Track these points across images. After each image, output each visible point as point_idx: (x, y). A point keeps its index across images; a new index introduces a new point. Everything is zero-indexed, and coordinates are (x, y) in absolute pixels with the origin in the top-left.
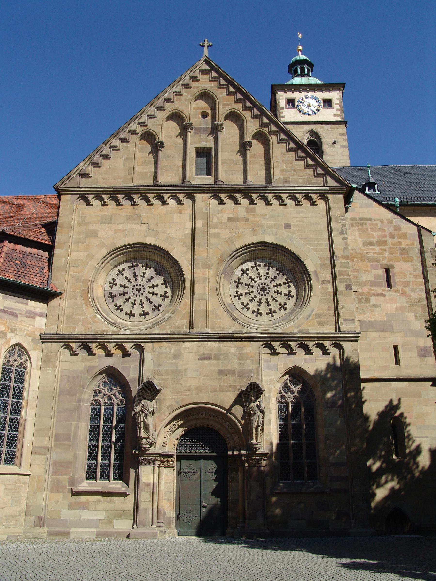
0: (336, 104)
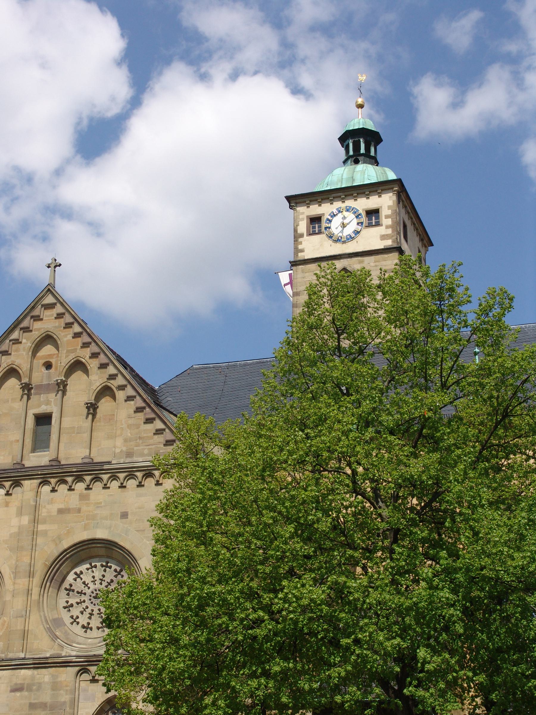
0: (387, 217)
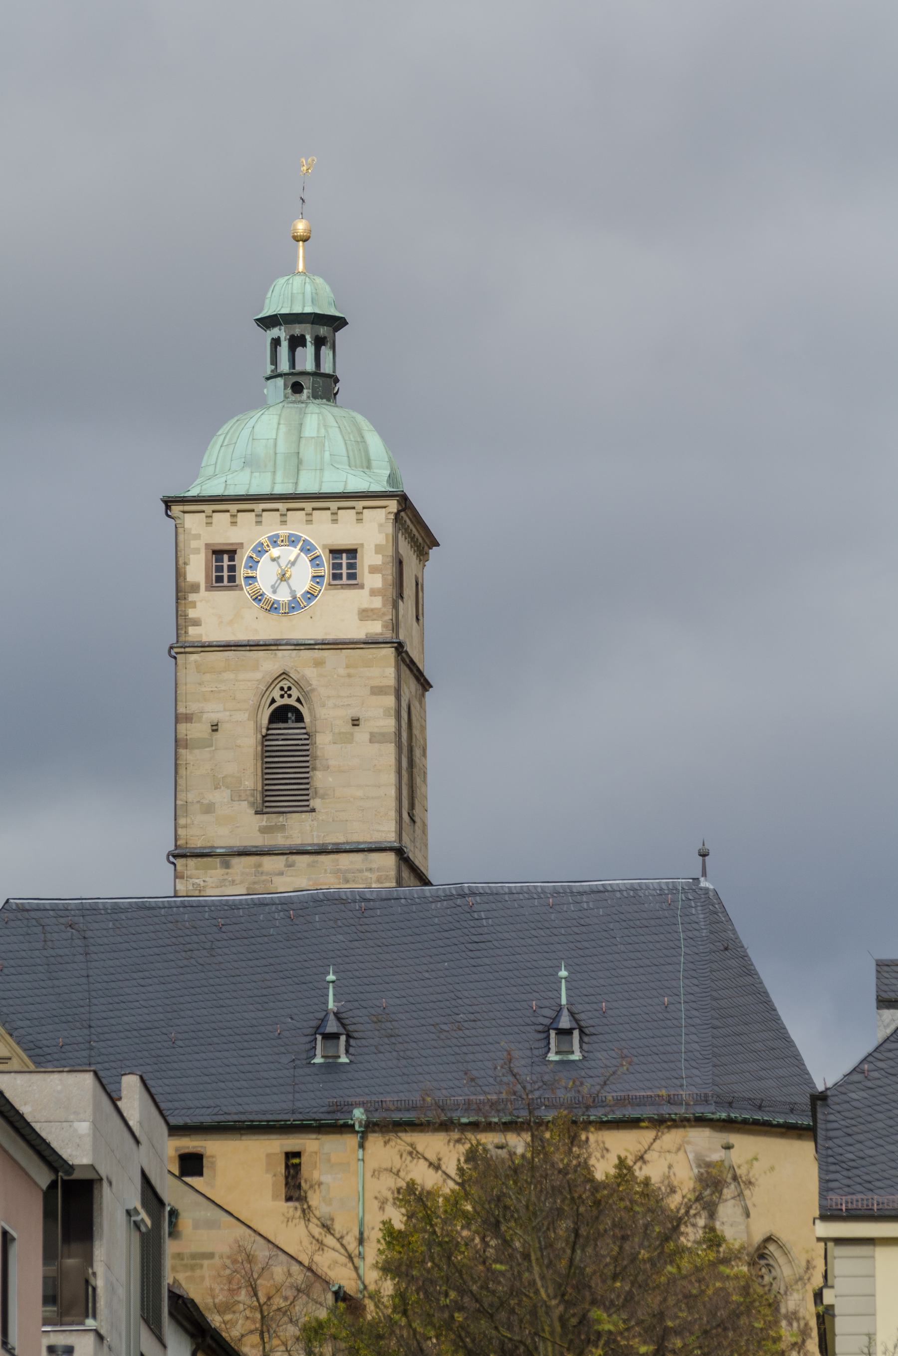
0: (373, 570)
